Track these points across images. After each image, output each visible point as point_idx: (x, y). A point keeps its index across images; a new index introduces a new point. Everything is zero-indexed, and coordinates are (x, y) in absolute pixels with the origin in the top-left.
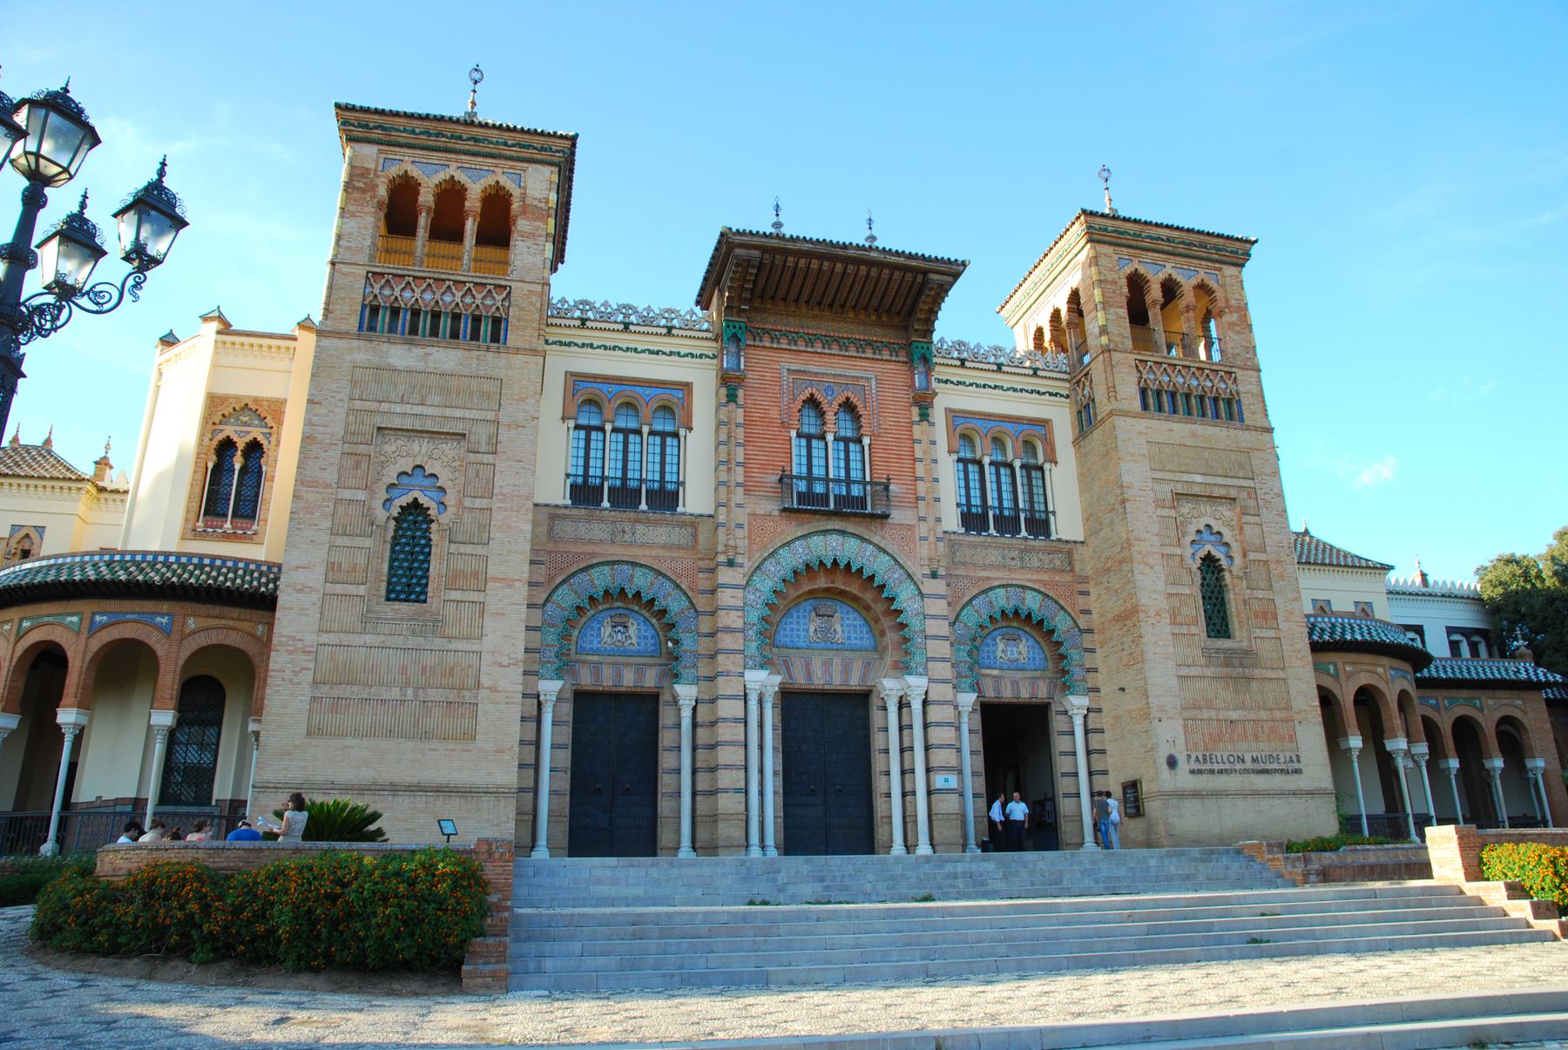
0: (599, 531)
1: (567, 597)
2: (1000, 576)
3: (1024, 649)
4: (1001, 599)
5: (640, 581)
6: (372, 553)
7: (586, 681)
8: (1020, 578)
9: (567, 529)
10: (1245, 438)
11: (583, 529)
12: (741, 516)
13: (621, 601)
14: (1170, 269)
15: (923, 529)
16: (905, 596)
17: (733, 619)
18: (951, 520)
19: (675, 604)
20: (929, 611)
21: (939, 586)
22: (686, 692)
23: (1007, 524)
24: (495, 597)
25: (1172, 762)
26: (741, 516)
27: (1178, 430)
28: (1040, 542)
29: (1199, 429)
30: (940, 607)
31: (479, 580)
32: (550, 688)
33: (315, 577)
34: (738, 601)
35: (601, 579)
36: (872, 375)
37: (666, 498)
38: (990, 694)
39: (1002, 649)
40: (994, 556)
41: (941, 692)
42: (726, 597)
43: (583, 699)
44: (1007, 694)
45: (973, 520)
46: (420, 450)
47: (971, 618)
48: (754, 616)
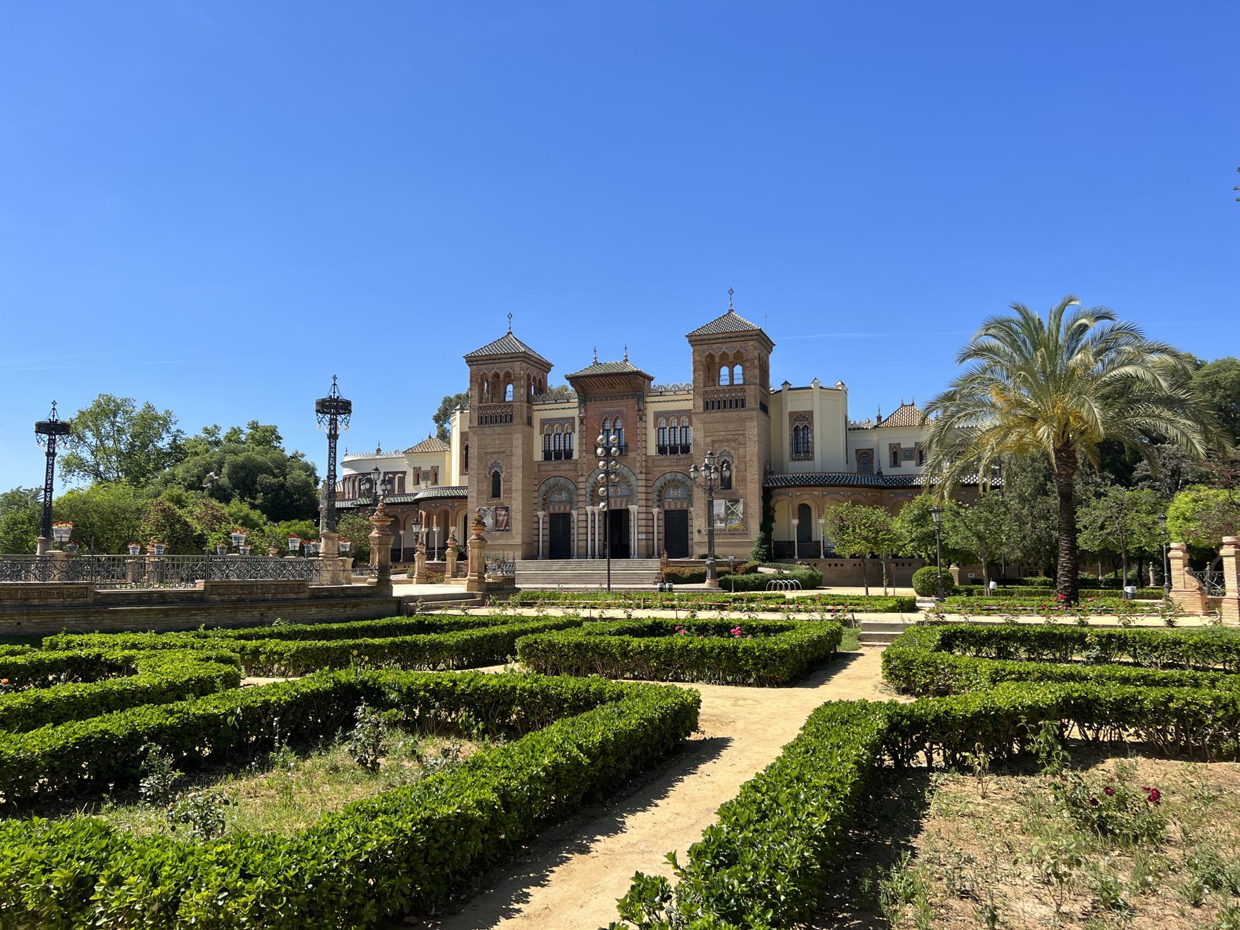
0: (551, 468)
1: (543, 488)
2: (669, 469)
3: (679, 493)
4: (668, 476)
5: (562, 481)
6: (487, 487)
7: (552, 511)
8: (675, 469)
9: (542, 468)
10: (744, 414)
11: (547, 468)
12: (585, 460)
13: (558, 488)
14: (724, 348)
15: (638, 458)
16: (632, 479)
17: (583, 492)
18: (652, 450)
19: (572, 487)
20: (639, 484)
21: (643, 476)
22: (574, 513)
23: (674, 450)
24: (514, 495)
25: (699, 531)
26: (585, 460)
27: (718, 415)
28: (684, 456)
29: (725, 414)
30: (643, 483)
31: (509, 491)
32: (541, 514)
33: (475, 494)
34: (584, 487)
35: (552, 481)
36: (626, 406)
37: (569, 455)
38: (667, 507)
39: (672, 493)
40: (667, 463)
41: (644, 509)
42: (581, 486)
43: (552, 515)
44: (673, 507)
45: (662, 450)
46: (495, 456)
47: (658, 484)
48: (588, 490)
